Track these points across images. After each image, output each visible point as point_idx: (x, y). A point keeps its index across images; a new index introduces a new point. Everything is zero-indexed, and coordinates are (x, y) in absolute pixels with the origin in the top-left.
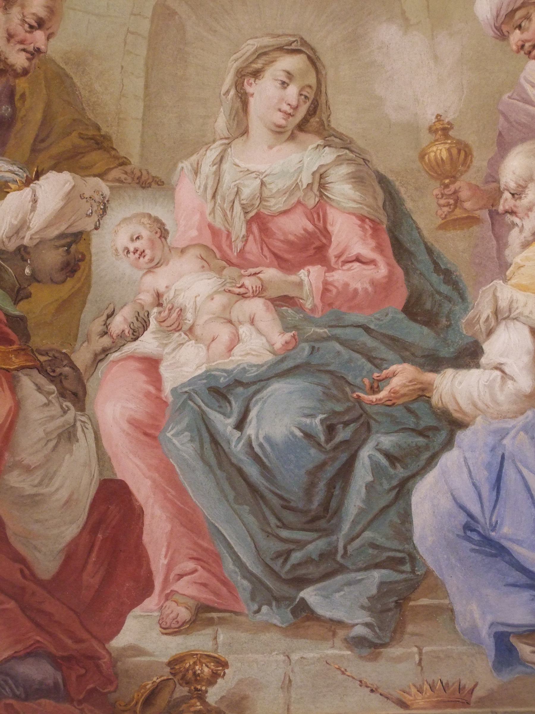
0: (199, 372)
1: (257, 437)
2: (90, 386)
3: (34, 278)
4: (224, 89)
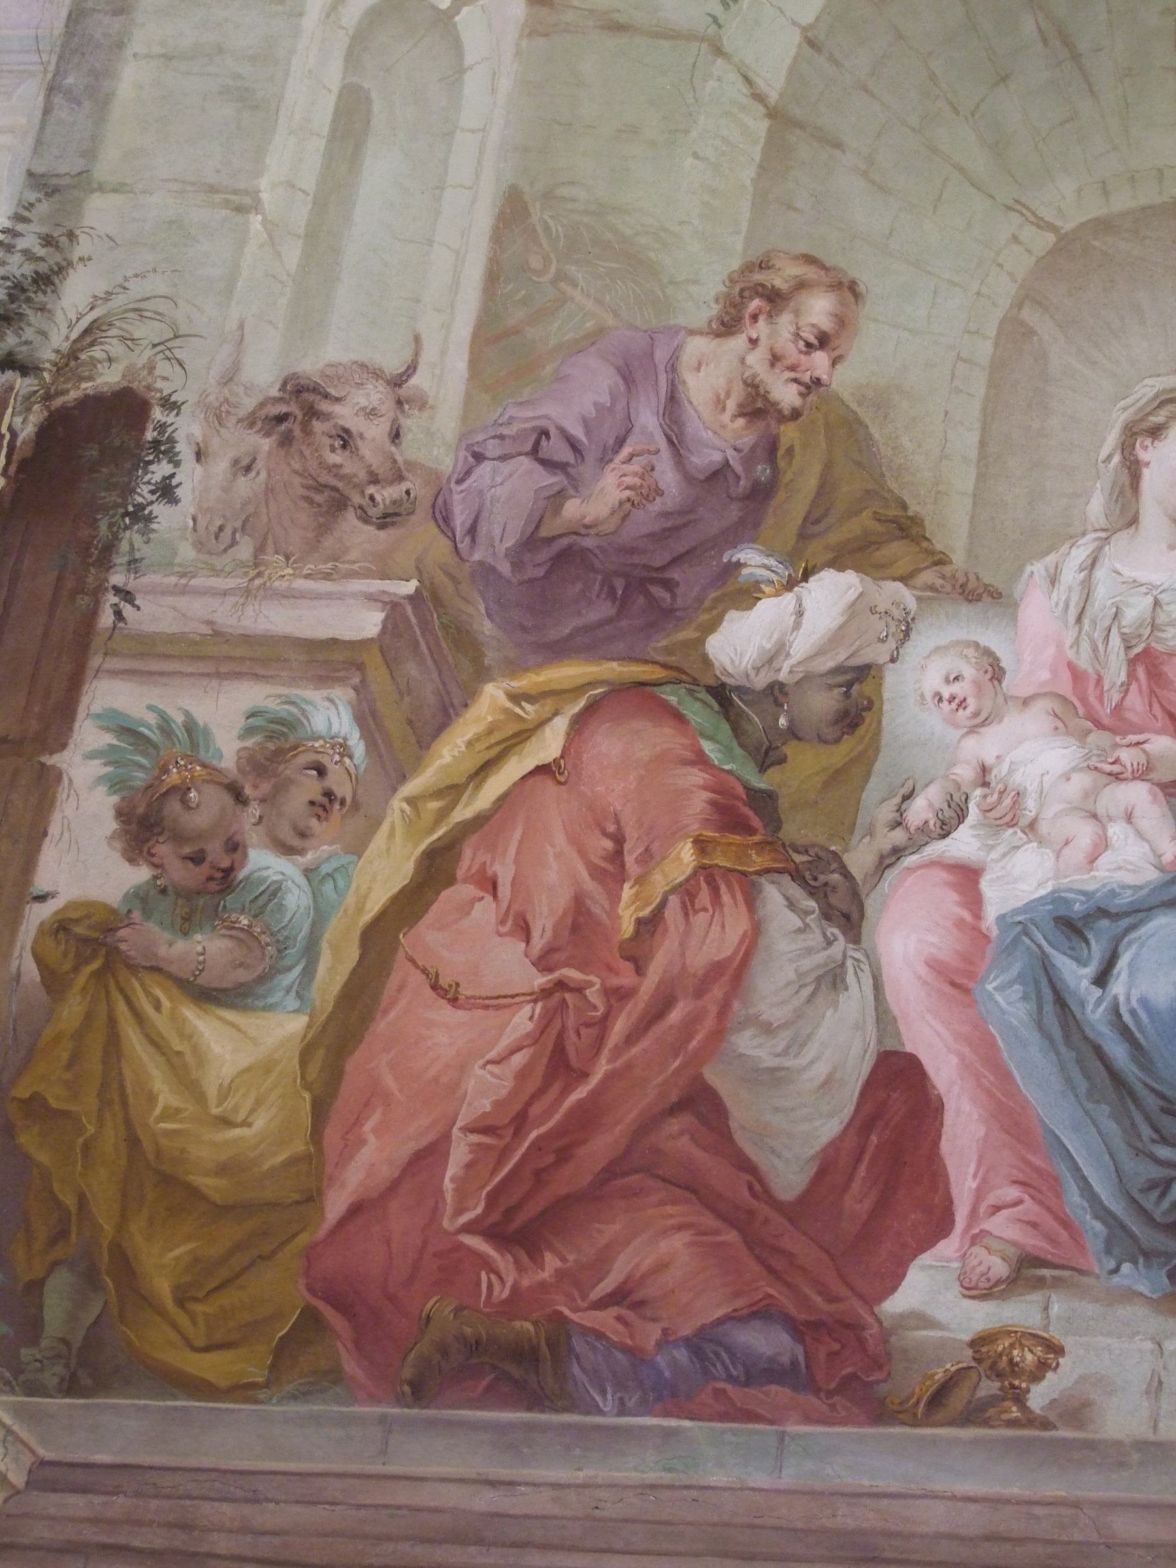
0: (1042, 892)
1: (1128, 999)
2: (871, 905)
3: (793, 733)
4: (1104, 454)
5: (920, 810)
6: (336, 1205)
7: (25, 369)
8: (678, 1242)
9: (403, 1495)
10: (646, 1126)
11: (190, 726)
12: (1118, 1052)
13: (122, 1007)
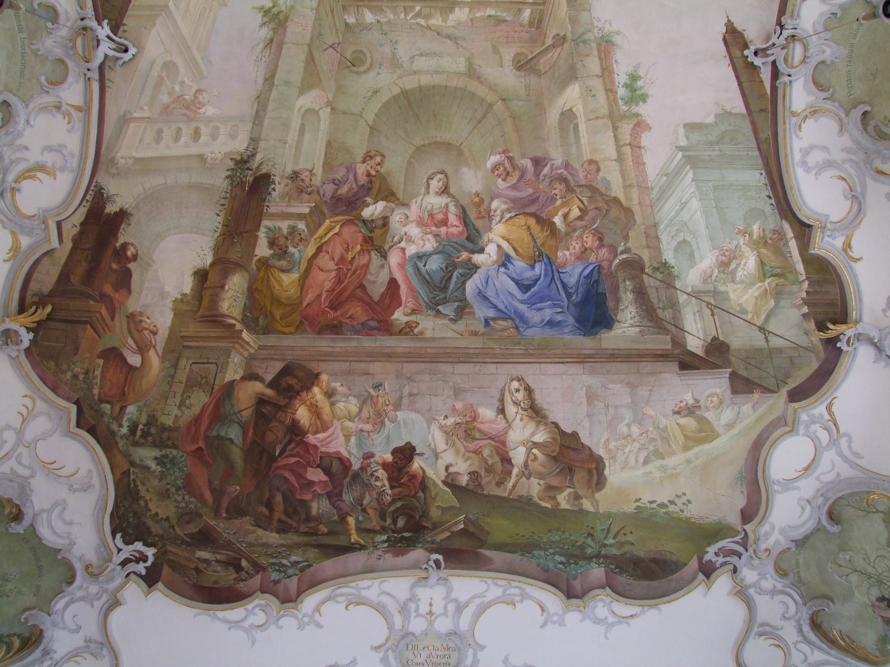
3: (375, 227)
5: (396, 239)
6: (305, 304)
7: (250, 170)
8: (359, 309)
9: (317, 349)
10: (353, 291)
11: (279, 227)
12: (427, 277)
13: (270, 274)
